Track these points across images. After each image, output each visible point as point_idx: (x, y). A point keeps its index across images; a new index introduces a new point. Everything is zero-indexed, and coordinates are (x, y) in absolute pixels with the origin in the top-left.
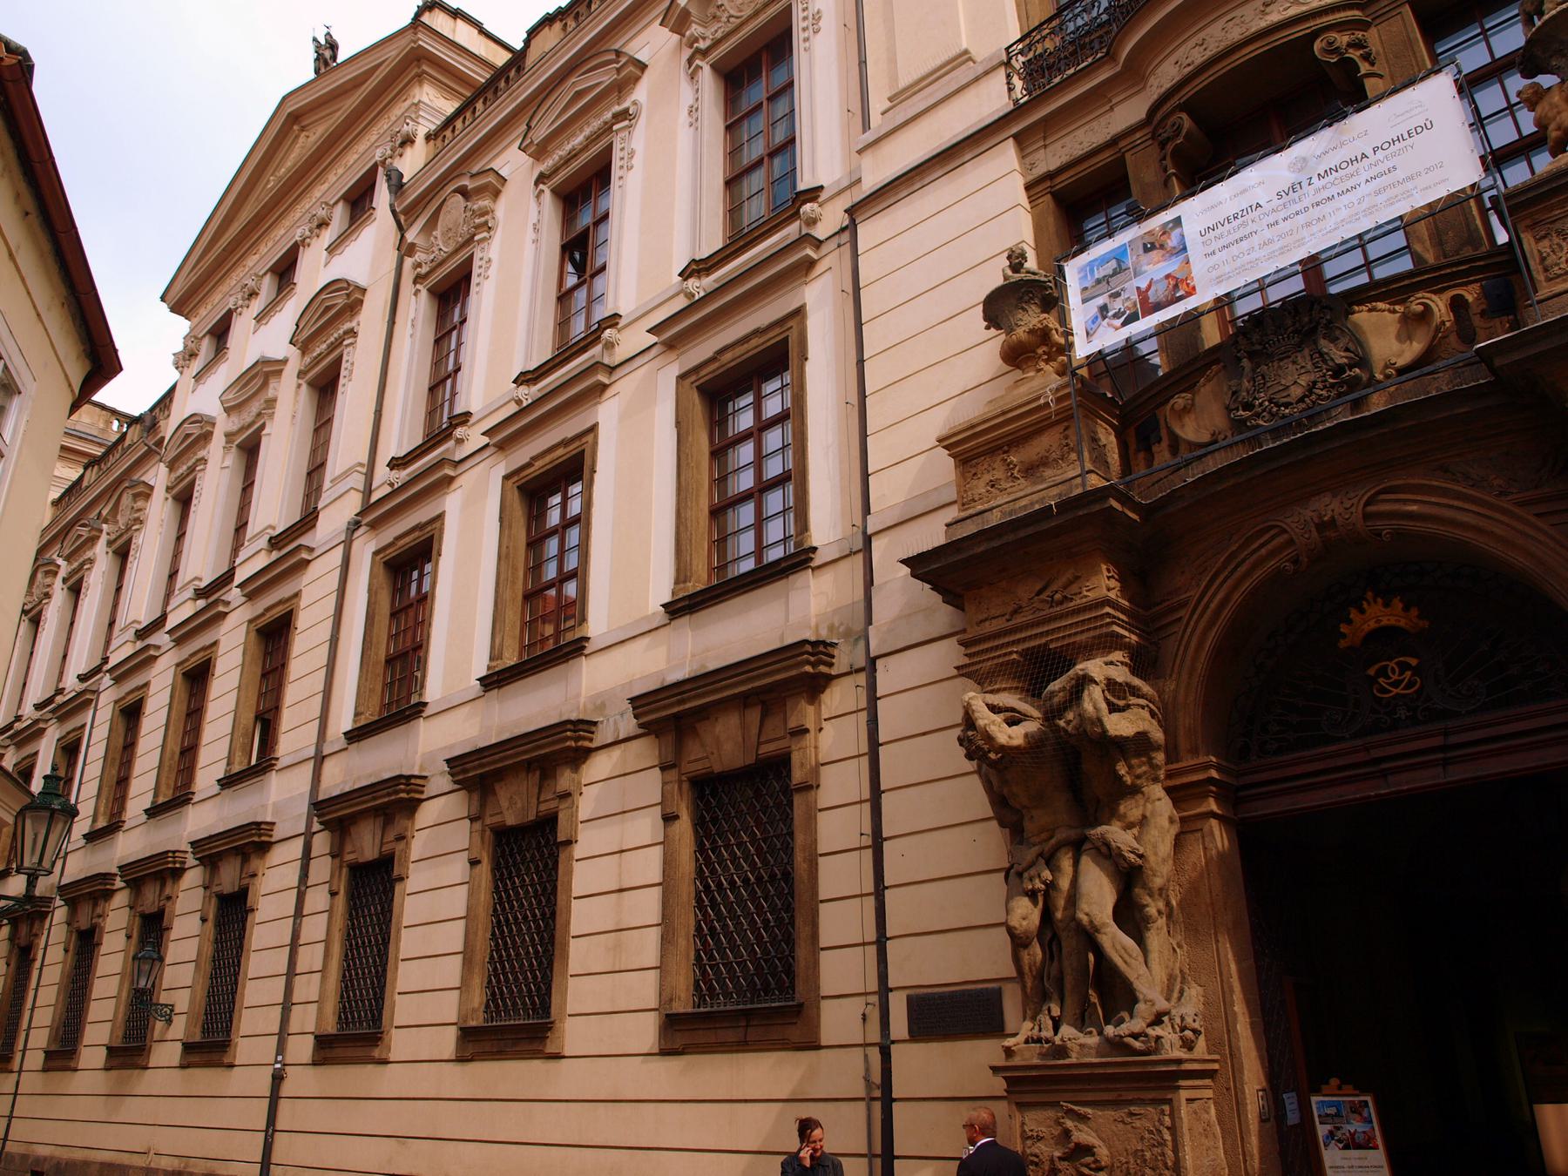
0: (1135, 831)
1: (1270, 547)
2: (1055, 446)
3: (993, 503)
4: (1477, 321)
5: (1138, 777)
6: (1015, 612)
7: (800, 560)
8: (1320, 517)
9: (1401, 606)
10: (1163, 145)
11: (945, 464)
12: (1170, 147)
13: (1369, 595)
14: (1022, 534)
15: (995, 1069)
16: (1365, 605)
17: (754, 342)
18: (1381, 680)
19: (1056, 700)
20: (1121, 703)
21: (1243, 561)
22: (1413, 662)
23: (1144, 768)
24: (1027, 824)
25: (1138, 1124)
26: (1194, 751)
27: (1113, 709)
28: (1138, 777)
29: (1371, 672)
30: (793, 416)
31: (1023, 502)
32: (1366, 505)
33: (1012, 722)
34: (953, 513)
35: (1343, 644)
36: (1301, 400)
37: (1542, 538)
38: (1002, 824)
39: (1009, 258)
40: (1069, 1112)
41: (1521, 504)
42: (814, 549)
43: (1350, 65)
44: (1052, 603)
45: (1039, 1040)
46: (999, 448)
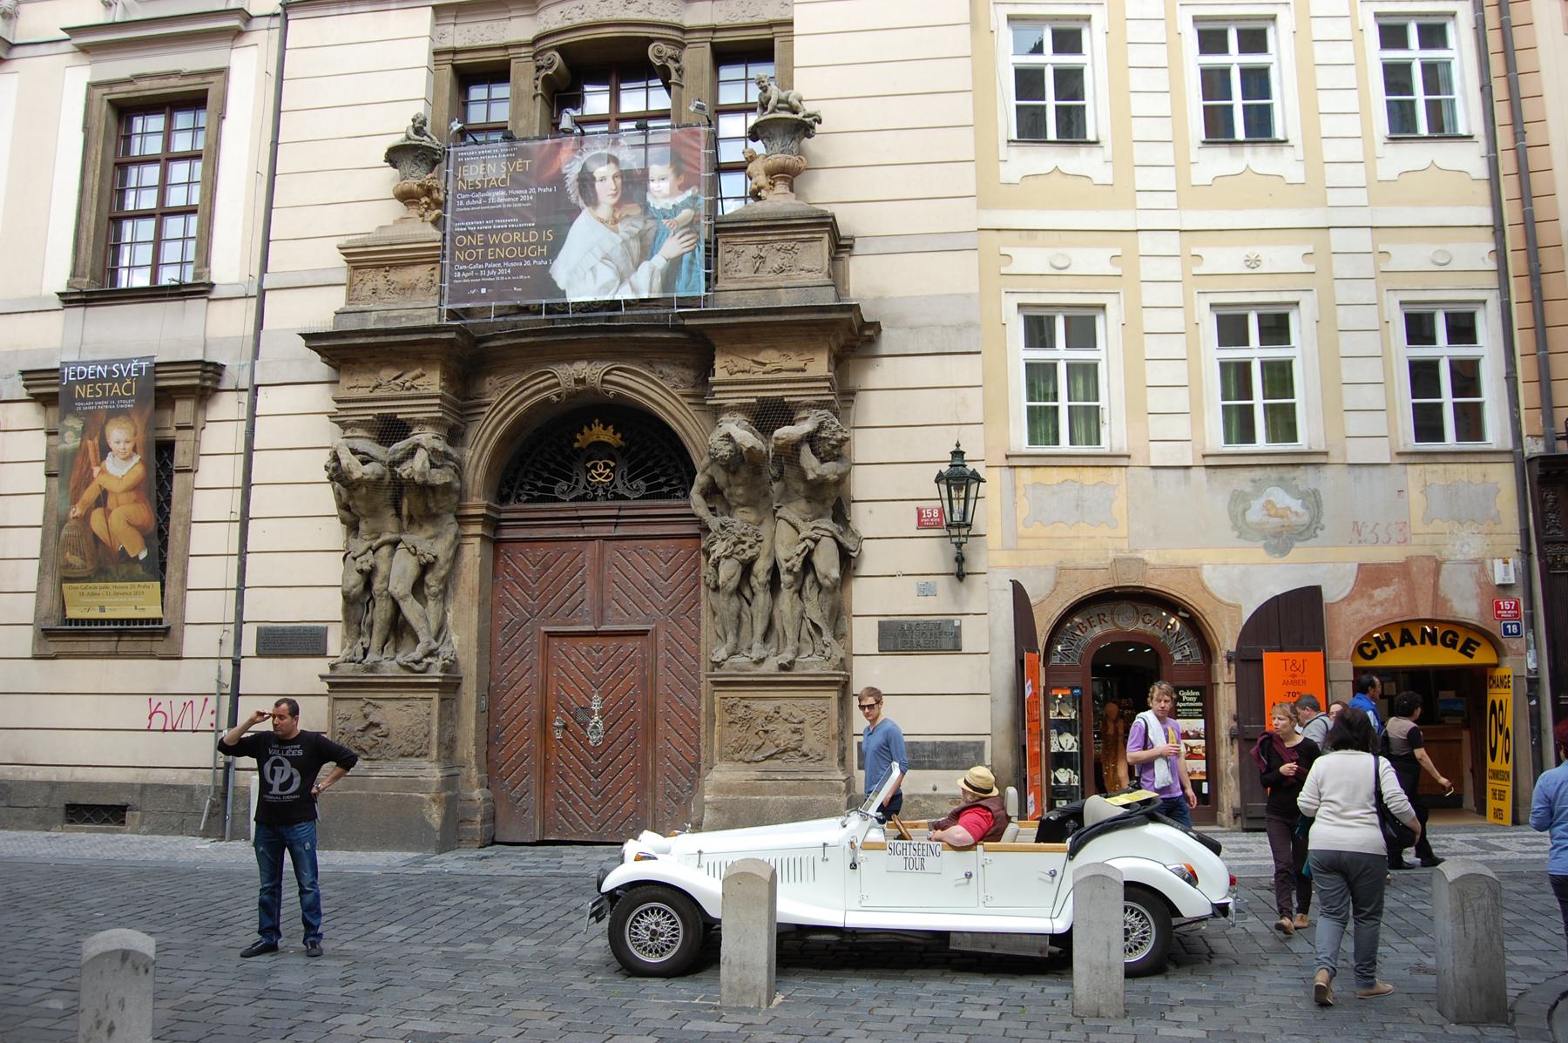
3: (371, 306)
7: (199, 290)
11: (340, 261)
12: (543, 73)
14: (392, 339)
15: (322, 677)
17: (173, 81)
19: (398, 456)
24: (362, 526)
30: (206, 157)
31: (395, 313)
33: (364, 462)
35: (576, 445)
38: (343, 522)
42: (212, 285)
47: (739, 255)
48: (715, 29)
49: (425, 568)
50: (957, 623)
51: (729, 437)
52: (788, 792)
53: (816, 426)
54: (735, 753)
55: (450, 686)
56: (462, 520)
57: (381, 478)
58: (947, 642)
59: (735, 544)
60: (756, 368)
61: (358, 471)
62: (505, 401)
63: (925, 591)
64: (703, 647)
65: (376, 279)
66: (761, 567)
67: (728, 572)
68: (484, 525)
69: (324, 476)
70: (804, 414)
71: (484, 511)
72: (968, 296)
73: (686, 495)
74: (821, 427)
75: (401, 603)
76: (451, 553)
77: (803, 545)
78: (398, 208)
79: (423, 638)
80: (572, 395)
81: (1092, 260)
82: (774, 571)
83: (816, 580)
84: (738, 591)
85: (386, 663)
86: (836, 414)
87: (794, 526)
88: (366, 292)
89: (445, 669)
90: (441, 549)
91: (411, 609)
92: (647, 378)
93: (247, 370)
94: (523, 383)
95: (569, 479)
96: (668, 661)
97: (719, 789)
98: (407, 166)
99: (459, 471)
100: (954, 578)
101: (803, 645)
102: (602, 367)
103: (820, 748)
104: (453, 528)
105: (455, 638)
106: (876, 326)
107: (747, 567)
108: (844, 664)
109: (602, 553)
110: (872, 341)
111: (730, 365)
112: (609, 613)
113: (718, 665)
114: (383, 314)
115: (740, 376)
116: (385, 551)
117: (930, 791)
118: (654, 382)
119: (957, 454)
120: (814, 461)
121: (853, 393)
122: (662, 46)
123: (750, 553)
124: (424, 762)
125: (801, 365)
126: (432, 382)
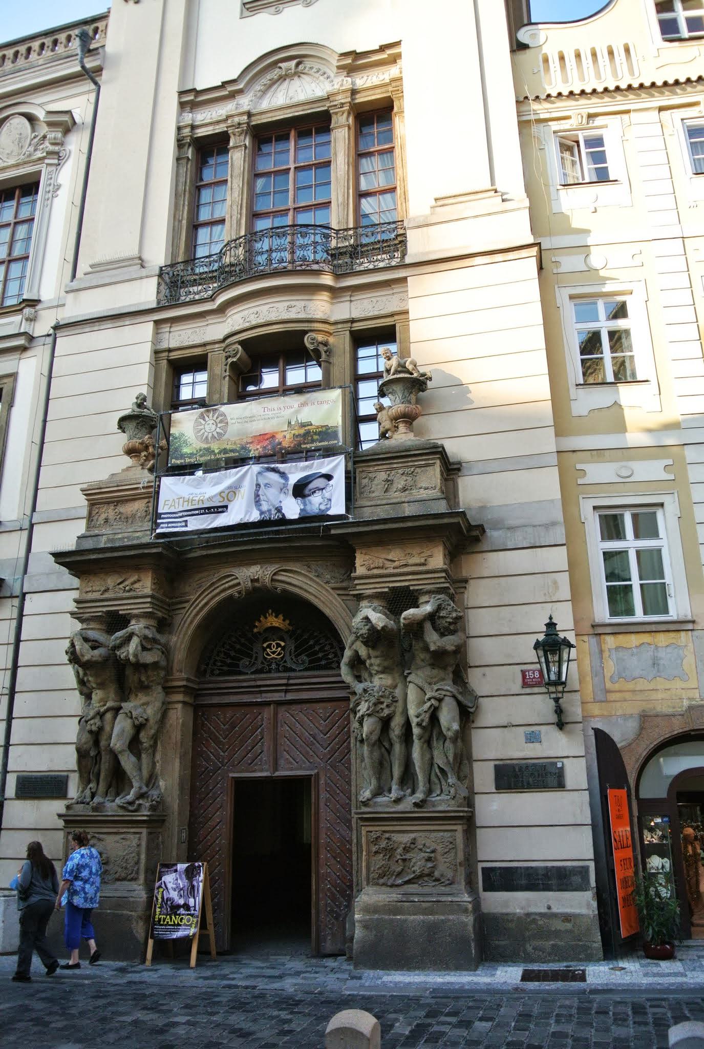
1: (230, 584)
5: (152, 681)
6: (107, 590)
10: (227, 358)
12: (230, 360)
14: (116, 554)
15: (60, 816)
19: (118, 642)
20: (149, 647)
22: (283, 644)
24: (93, 696)
25: (125, 843)
28: (152, 681)
29: (265, 645)
31: (120, 536)
32: (274, 574)
33: (93, 648)
35: (255, 630)
38: (81, 693)
40: (94, 837)
41: (333, 589)
44: (124, 591)
45: (83, 803)
46: (113, 502)
47: (372, 480)
48: (353, 321)
49: (139, 728)
50: (559, 765)
51: (367, 619)
52: (425, 912)
53: (435, 607)
54: (382, 878)
55: (157, 822)
56: (168, 690)
58: (552, 780)
59: (375, 704)
60: (388, 564)
61: (89, 654)
62: (201, 599)
63: (533, 738)
64: (353, 789)
65: (109, 512)
68: (184, 692)
69: (65, 659)
71: (184, 683)
72: (552, 501)
73: (339, 667)
74: (439, 608)
75: (120, 757)
77: (428, 704)
78: (128, 461)
79: (136, 784)
80: (248, 593)
83: (440, 732)
84: (379, 741)
85: (108, 805)
86: (452, 597)
88: (101, 520)
89: (153, 808)
90: (150, 711)
91: (128, 762)
92: (305, 576)
93: (19, 582)
94: (213, 584)
95: (251, 657)
96: (327, 800)
97: (367, 909)
99: (166, 651)
100: (554, 727)
101: (433, 787)
102: (271, 569)
103: (449, 874)
105: (162, 783)
106: (481, 528)
107: (386, 723)
108: (469, 802)
109: (276, 714)
112: (282, 762)
113: (365, 804)
114: (111, 537)
115: (376, 572)
116: (109, 716)
117: (546, 910)
118: (311, 579)
119: (551, 625)
121: (466, 581)
123: (386, 712)
124: (134, 885)
125: (423, 560)
126: (146, 585)
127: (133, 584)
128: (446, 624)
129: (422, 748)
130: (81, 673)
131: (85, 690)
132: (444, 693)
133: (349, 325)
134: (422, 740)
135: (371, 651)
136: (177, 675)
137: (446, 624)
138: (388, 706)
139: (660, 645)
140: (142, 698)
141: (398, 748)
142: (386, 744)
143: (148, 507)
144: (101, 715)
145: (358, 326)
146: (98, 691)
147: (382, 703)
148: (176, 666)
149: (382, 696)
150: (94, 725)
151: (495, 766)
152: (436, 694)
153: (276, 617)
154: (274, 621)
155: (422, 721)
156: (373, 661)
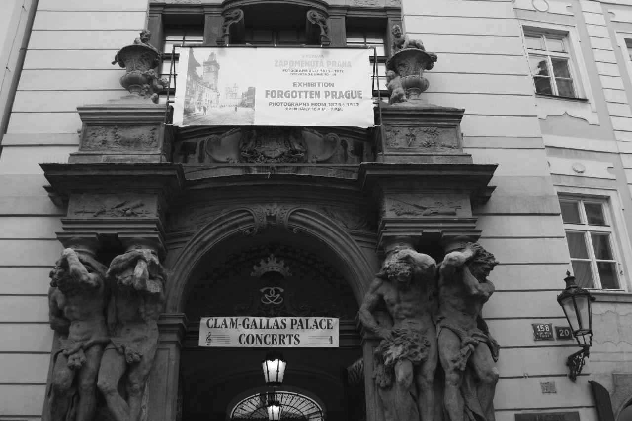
0: (138, 343)
2: (146, 135)
4: (349, 154)
5: (148, 315)
6: (101, 213)
8: (270, 213)
9: (283, 264)
10: (227, 20)
11: (77, 123)
12: (230, 22)
13: (272, 255)
16: (269, 259)
18: (266, 295)
20: (153, 275)
21: (226, 223)
22: (282, 290)
23: (151, 312)
24: (73, 329)
26: (174, 309)
27: (151, 278)
29: (262, 290)
32: (292, 214)
34: (75, 150)
35: (252, 274)
36: (276, 158)
37: (356, 250)
38: (53, 327)
39: (141, 34)
41: (352, 234)
43: (316, 27)
44: (124, 214)
47: (396, 133)
48: (348, 8)
49: (130, 366)
51: (407, 259)
56: (163, 328)
57: (98, 287)
59: (410, 348)
60: (418, 211)
63: (548, 389)
66: (430, 367)
67: (403, 371)
70: (458, 246)
71: (181, 322)
76: (152, 355)
77: (466, 349)
80: (261, 231)
81: (595, 169)
82: (440, 372)
87: (457, 334)
90: (146, 350)
92: (323, 219)
94: (221, 219)
98: (134, 62)
100: (567, 379)
104: (157, 333)
110: (485, 200)
111: (397, 208)
115: (406, 216)
116: (95, 351)
118: (329, 223)
120: (477, 282)
122: (316, 13)
123: (421, 356)
125: (453, 210)
126: (151, 211)
127: (135, 208)
128: (482, 271)
129: (457, 395)
130: (60, 302)
131: (61, 323)
132: (479, 339)
133: (345, 12)
134: (458, 386)
135: (402, 295)
136: (170, 313)
137: (482, 271)
138: (422, 351)
139: (621, 314)
140: (139, 333)
141: (429, 395)
142: (414, 392)
143: (153, 133)
144: (86, 350)
145: (353, 14)
146: (80, 323)
147: (416, 347)
148: (170, 304)
149: (416, 340)
150: (77, 360)
151: (516, 415)
152: (472, 339)
153: (277, 262)
154: (273, 265)
155: (461, 365)
156: (404, 304)
